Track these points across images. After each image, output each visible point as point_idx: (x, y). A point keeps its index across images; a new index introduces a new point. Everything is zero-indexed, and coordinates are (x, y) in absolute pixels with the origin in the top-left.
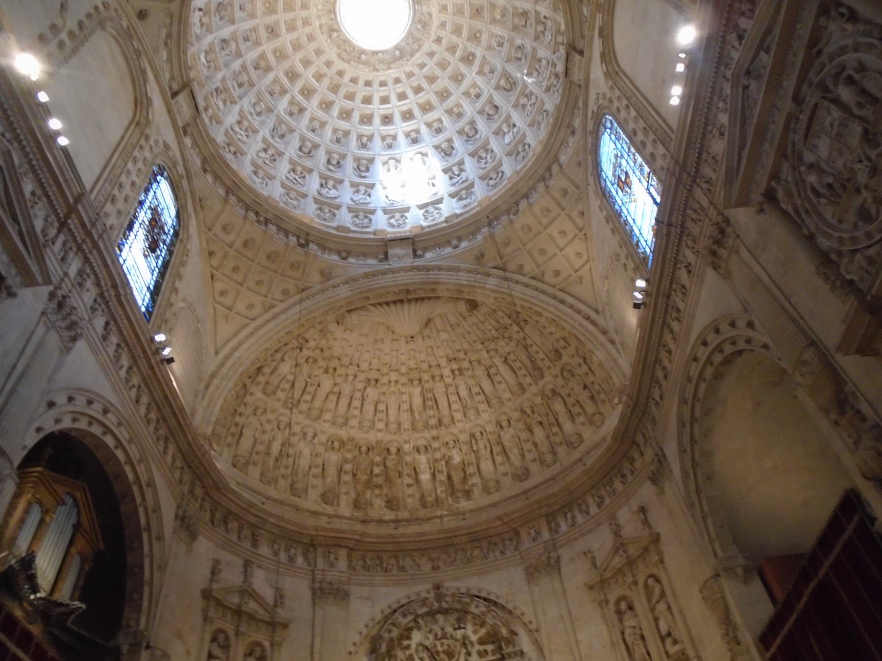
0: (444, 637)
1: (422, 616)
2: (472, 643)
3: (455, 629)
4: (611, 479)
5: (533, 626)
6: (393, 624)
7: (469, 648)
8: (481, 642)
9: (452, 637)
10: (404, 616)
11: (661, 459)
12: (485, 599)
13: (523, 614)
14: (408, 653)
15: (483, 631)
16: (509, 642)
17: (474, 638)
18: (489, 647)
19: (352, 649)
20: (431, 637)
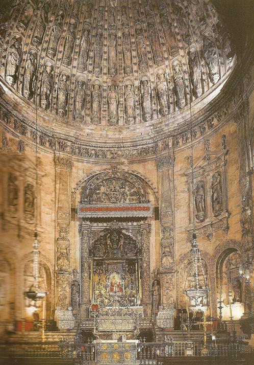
0: (115, 191)
1: (106, 180)
2: (127, 195)
3: (120, 188)
4: (213, 118)
5: (156, 190)
6: (93, 183)
7: (126, 196)
8: (131, 195)
9: (118, 191)
10: (97, 179)
11: (245, 105)
12: (136, 176)
13: (152, 184)
14: (98, 196)
15: (132, 191)
16: (143, 196)
17: (128, 193)
18: (134, 197)
19: (73, 190)
20: (109, 190)
